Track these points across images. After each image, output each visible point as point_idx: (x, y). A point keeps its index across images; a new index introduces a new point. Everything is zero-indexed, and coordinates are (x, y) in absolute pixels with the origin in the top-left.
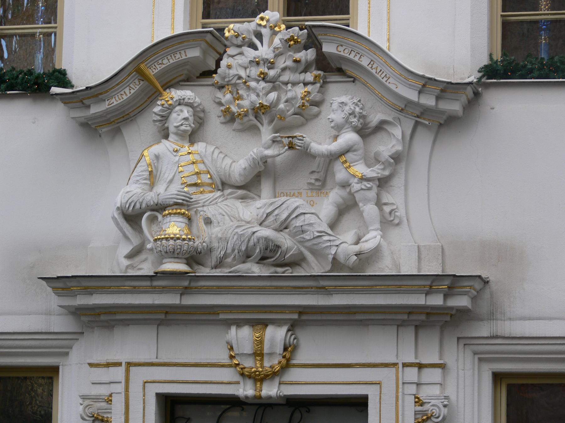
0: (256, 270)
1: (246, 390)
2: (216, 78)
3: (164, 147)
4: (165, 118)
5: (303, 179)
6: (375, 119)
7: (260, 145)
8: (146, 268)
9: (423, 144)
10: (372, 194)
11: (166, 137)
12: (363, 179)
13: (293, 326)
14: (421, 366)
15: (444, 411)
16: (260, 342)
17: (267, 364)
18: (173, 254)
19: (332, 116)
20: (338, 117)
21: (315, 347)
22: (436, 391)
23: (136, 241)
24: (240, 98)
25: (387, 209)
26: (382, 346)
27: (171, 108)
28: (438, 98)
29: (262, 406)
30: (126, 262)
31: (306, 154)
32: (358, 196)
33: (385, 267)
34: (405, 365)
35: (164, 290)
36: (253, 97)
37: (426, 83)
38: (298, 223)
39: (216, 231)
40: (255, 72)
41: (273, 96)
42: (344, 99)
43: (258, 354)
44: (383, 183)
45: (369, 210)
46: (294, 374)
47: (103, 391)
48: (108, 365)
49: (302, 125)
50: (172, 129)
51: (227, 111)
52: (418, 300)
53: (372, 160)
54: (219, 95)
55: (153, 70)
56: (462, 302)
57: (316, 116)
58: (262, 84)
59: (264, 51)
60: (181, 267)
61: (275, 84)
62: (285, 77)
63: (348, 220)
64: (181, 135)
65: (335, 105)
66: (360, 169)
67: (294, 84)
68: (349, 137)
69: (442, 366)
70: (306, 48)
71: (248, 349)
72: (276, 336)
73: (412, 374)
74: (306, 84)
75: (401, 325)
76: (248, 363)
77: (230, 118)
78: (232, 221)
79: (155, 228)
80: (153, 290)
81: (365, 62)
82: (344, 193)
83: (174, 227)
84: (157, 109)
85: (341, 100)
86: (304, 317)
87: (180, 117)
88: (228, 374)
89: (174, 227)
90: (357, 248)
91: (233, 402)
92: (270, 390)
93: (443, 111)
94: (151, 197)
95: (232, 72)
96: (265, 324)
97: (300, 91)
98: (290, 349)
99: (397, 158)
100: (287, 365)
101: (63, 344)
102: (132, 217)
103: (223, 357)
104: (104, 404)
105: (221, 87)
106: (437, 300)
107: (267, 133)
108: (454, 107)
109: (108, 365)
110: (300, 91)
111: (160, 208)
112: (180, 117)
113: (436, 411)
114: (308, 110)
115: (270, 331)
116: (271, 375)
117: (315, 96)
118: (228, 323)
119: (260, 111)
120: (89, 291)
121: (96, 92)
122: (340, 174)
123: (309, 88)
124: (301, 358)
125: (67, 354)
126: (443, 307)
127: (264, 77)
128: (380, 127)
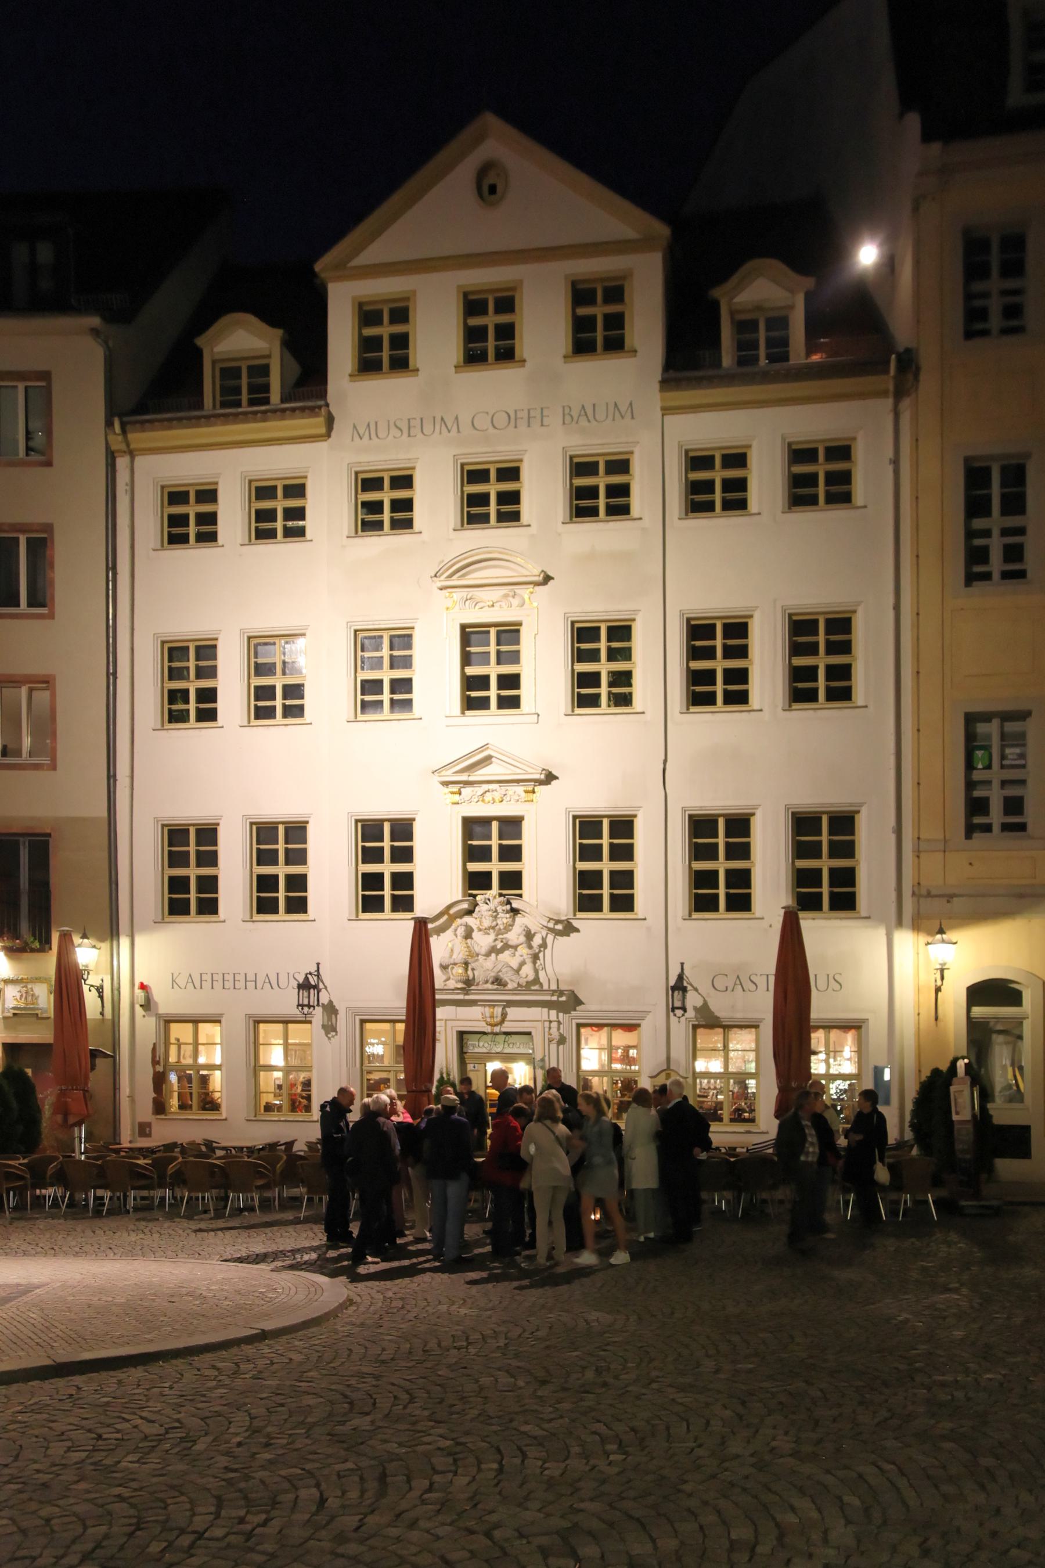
0: (489, 986)
2: (474, 915)
4: (456, 930)
21: (513, 1012)
46: (506, 1024)
55: (452, 911)
71: (488, 1015)
76: (488, 1020)
96: (494, 1006)
98: (504, 1015)
103: (480, 1017)
116: (496, 1025)
124: (508, 1018)
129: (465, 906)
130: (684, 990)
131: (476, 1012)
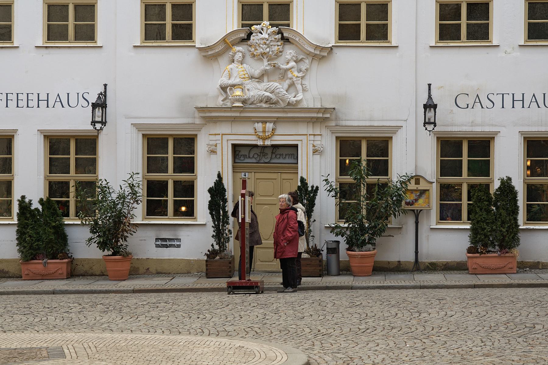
0: (264, 105)
1: (260, 143)
2: (249, 43)
3: (233, 66)
5: (276, 77)
6: (301, 57)
7: (265, 65)
8: (229, 105)
9: (315, 65)
10: (300, 82)
11: (233, 62)
12: (297, 77)
13: (275, 123)
14: (314, 135)
15: (322, 149)
16: (265, 128)
17: (267, 134)
18: (238, 100)
19: (287, 57)
20: (289, 57)
21: (281, 129)
22: (319, 143)
23: (225, 96)
24: (257, 50)
25: (304, 86)
26: (303, 129)
27: (235, 53)
28: (320, 51)
29: (264, 147)
30: (222, 103)
31: (279, 68)
32: (295, 82)
33: (305, 105)
35: (235, 111)
36: (262, 50)
37: (317, 47)
38: (278, 91)
39: (252, 93)
40: (262, 42)
41: (268, 50)
42: (291, 51)
43: (264, 131)
44: (302, 78)
45: (299, 87)
46: (275, 138)
47: (214, 143)
48: (215, 135)
49: (277, 58)
50: (235, 60)
51: (253, 54)
52: (315, 115)
53: (300, 71)
54: (250, 48)
56: (328, 115)
57: (281, 55)
58: (264, 46)
59: (265, 35)
60: (241, 105)
61: (269, 46)
62: (272, 44)
63: (292, 89)
64: (238, 62)
65: (288, 53)
66: (296, 74)
67: (274, 46)
68: (292, 64)
69: (321, 135)
70: (278, 34)
72: (269, 126)
73: (312, 138)
74: (278, 46)
76: (261, 134)
77: (253, 56)
78: (256, 91)
79: (231, 92)
80: (231, 111)
81: (297, 39)
82: (290, 81)
83: (238, 92)
84: (231, 53)
85: (289, 52)
87: (238, 56)
88: (254, 138)
89: (238, 92)
90: (295, 99)
91: (256, 146)
92: (268, 143)
93: (321, 54)
94: (231, 82)
95: (254, 41)
96: (266, 122)
97: (276, 48)
99: (307, 70)
100: (273, 134)
101: (199, 128)
102: (224, 88)
103: (253, 132)
105: (250, 46)
106: (320, 115)
107: (265, 60)
108: (325, 54)
109: (215, 135)
110: (276, 48)
111: (234, 86)
112: (238, 56)
113: (319, 149)
114: (278, 54)
115: (268, 124)
117: (281, 50)
118: (254, 122)
119: (263, 54)
120: (210, 112)
121: (210, 48)
122: (290, 75)
123: (279, 47)
124: (277, 132)
126: (321, 117)
127: (265, 44)
128: (301, 60)
129: (243, 35)
130: (435, 107)
131: (248, 129)
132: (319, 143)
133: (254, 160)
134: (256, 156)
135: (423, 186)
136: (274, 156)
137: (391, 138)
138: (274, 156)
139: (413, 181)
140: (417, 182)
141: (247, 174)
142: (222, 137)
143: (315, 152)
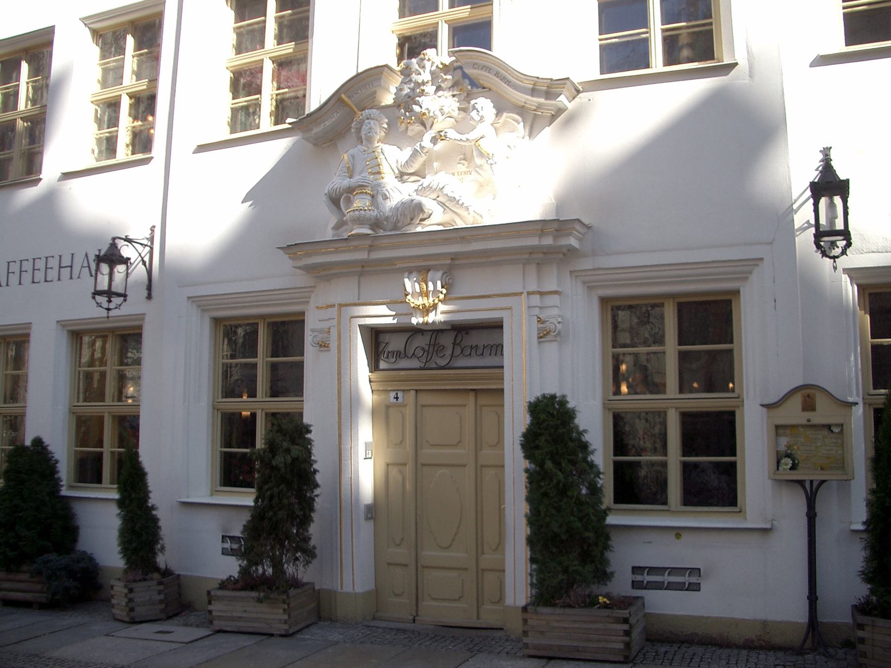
14: (542, 294)
15: (559, 326)
22: (555, 312)
26: (511, 280)
34: (529, 293)
47: (324, 325)
52: (533, 241)
73: (536, 300)
75: (526, 263)
83: (360, 203)
86: (457, 262)
102: (335, 200)
104: (326, 335)
106: (548, 241)
113: (552, 326)
125: (308, 302)
132: (555, 312)
133: (415, 363)
134: (419, 353)
135: (823, 414)
136: (458, 351)
137: (737, 293)
138: (458, 351)
139: (797, 402)
140: (809, 405)
141: (400, 395)
142: (340, 310)
143: (543, 335)
